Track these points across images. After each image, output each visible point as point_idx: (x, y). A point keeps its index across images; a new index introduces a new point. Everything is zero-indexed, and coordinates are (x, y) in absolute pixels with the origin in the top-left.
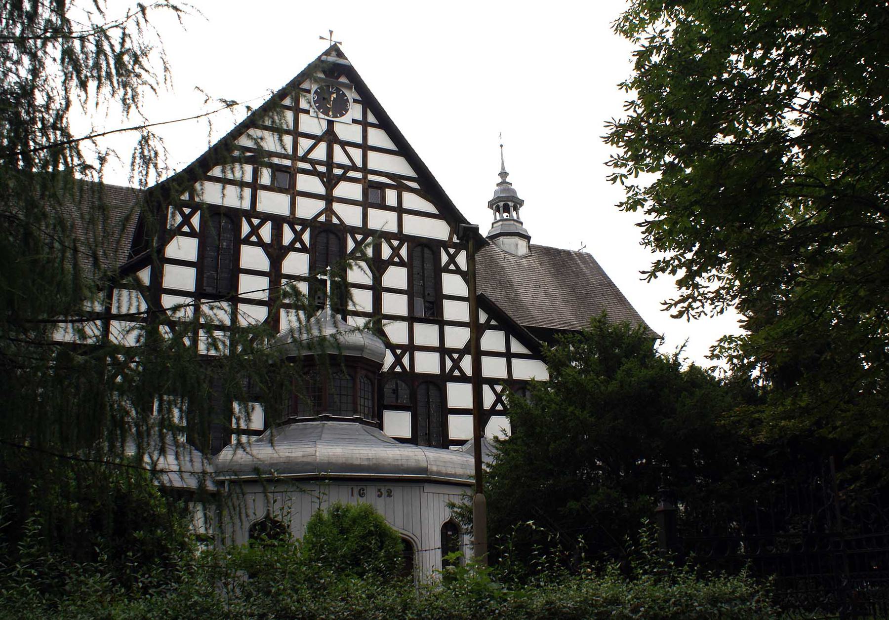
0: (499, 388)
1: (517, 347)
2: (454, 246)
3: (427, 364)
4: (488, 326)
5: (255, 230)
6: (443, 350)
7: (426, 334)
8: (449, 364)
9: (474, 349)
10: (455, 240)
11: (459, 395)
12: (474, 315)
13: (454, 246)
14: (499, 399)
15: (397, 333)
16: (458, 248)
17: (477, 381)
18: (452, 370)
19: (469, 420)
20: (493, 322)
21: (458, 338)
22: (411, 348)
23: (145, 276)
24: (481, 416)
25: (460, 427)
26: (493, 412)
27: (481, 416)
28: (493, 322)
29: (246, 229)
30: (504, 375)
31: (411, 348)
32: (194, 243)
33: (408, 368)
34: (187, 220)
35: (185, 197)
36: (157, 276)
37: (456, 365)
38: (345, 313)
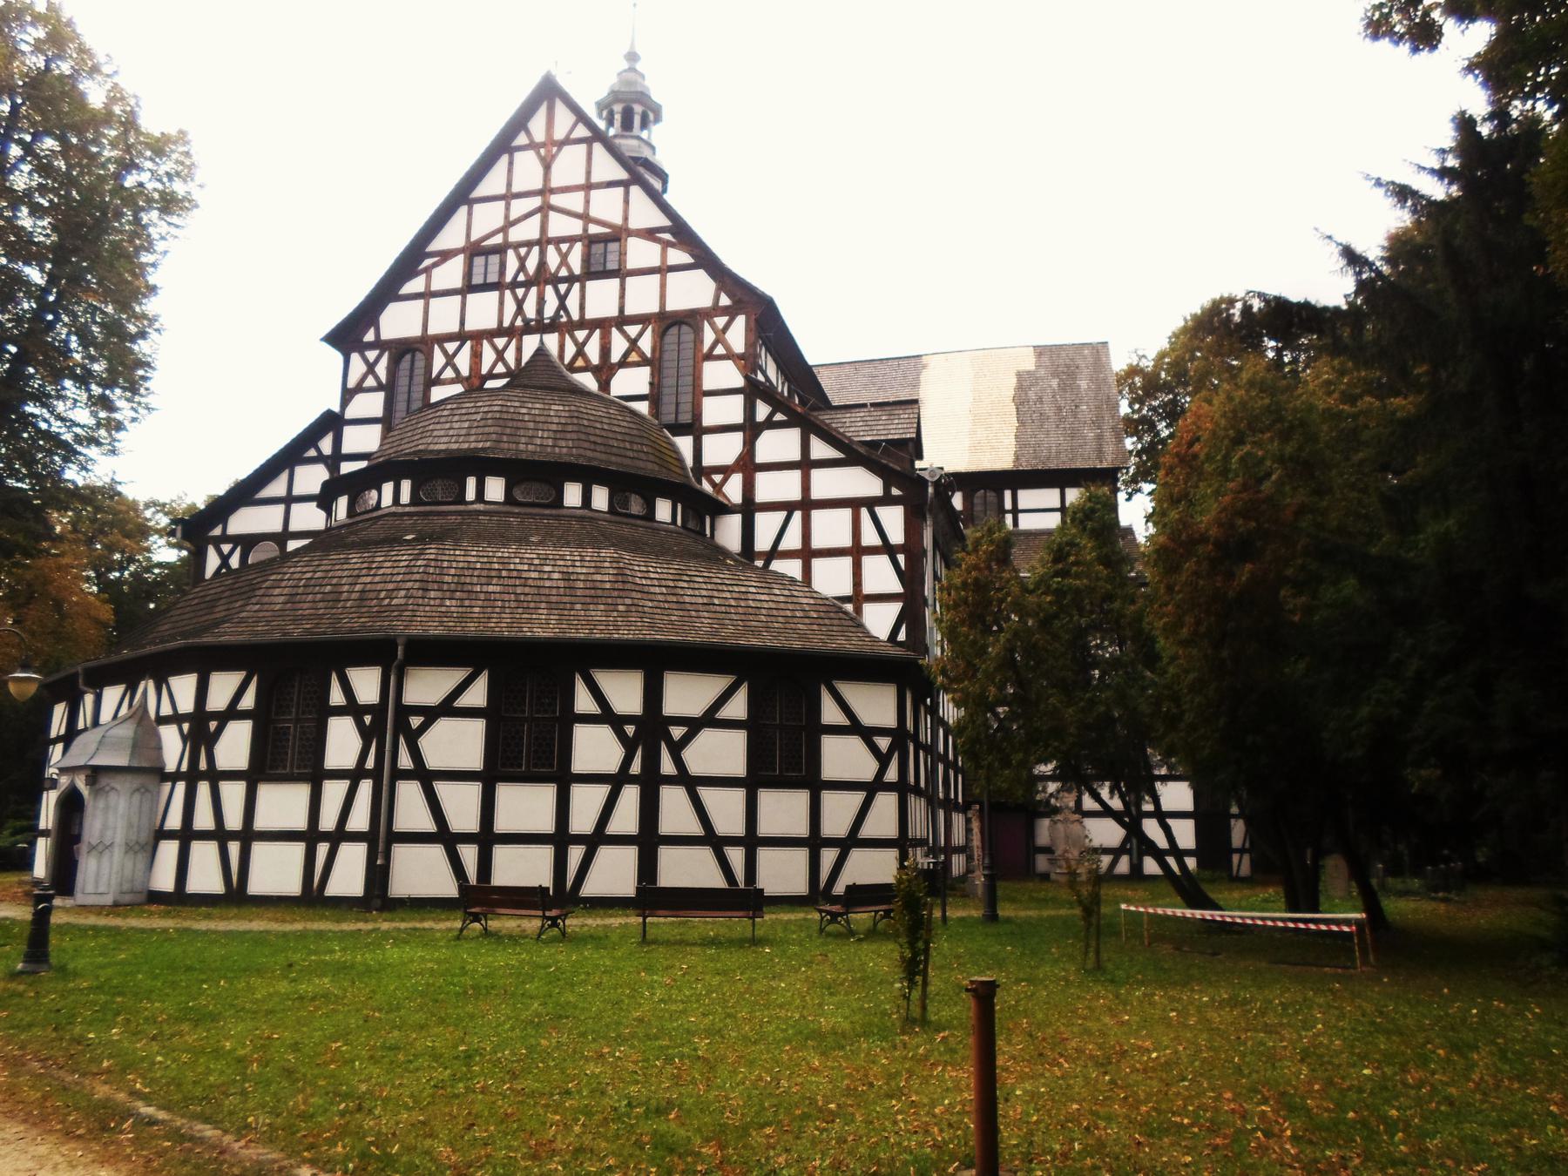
1: (820, 449)
2: (725, 311)
4: (770, 424)
5: (450, 360)
10: (725, 301)
12: (750, 410)
13: (725, 311)
16: (731, 313)
20: (779, 417)
23: (326, 445)
28: (779, 417)
29: (439, 360)
32: (381, 396)
34: (371, 368)
35: (370, 336)
36: (337, 442)
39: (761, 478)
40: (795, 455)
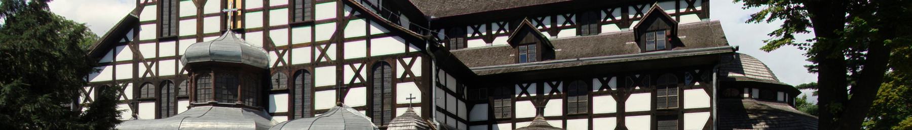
0: (357, 66)
3: (301, 57)
6: (313, 44)
7: (302, 34)
8: (318, 53)
9: (339, 39)
11: (325, 76)
14: (357, 74)
15: (279, 38)
17: (340, 63)
18: (320, 58)
19: (333, 93)
21: (325, 32)
22: (290, 47)
24: (341, 90)
25: (325, 100)
26: (352, 85)
27: (341, 90)
30: (363, 54)
31: (290, 47)
33: (287, 62)
37: (323, 53)
38: (242, 31)
39: (347, 45)
40: (364, 34)
